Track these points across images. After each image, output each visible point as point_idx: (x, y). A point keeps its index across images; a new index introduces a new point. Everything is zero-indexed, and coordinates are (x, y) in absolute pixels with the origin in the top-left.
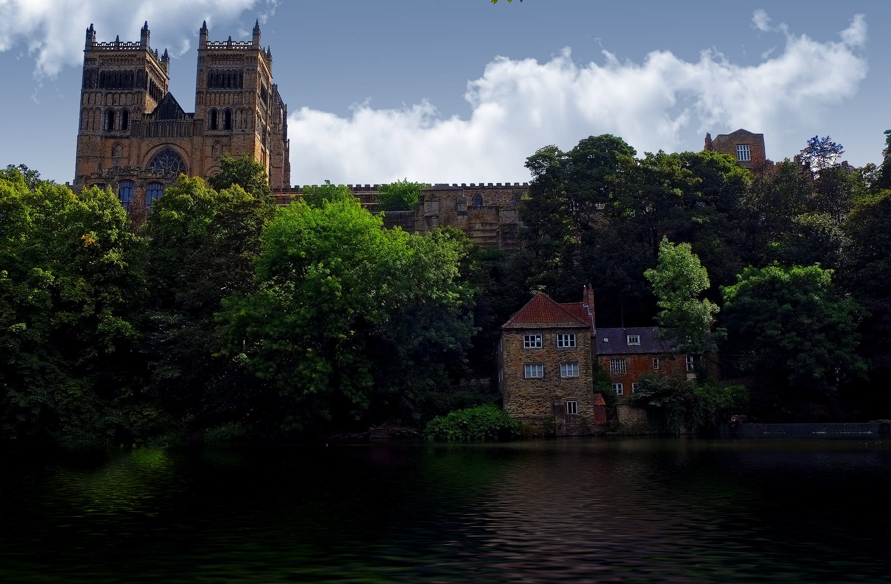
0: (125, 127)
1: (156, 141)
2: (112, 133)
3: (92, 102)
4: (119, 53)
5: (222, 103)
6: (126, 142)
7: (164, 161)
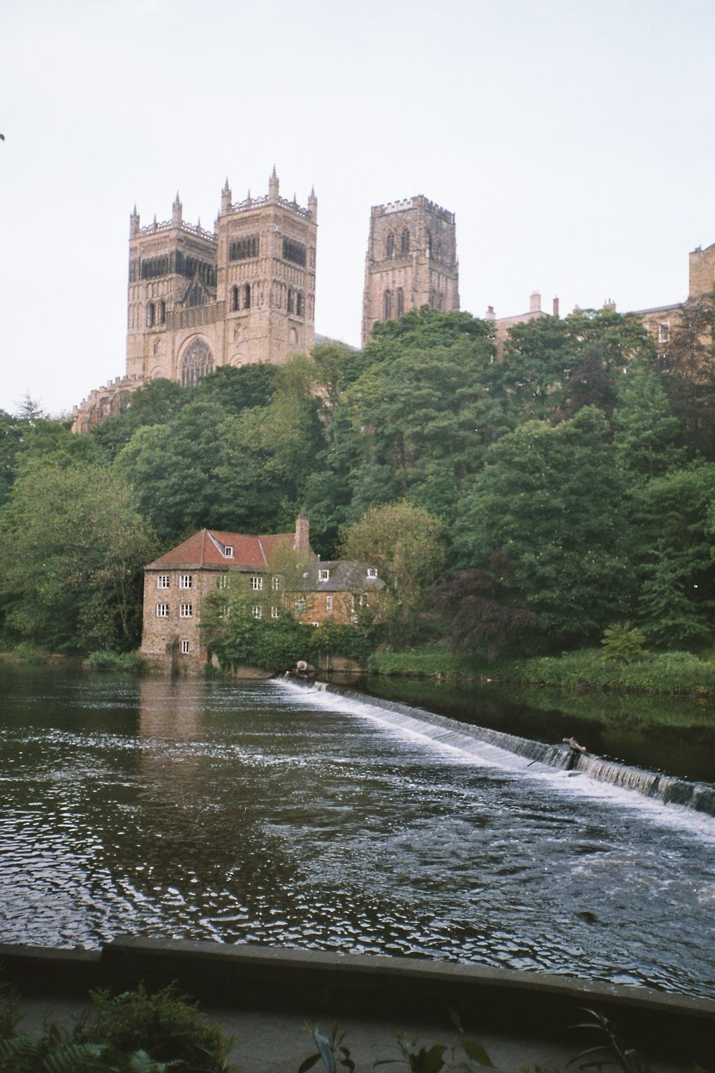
0: (163, 320)
1: (187, 332)
2: (153, 329)
3: (136, 296)
4: (155, 237)
5: (242, 276)
6: (163, 336)
7: (195, 353)
